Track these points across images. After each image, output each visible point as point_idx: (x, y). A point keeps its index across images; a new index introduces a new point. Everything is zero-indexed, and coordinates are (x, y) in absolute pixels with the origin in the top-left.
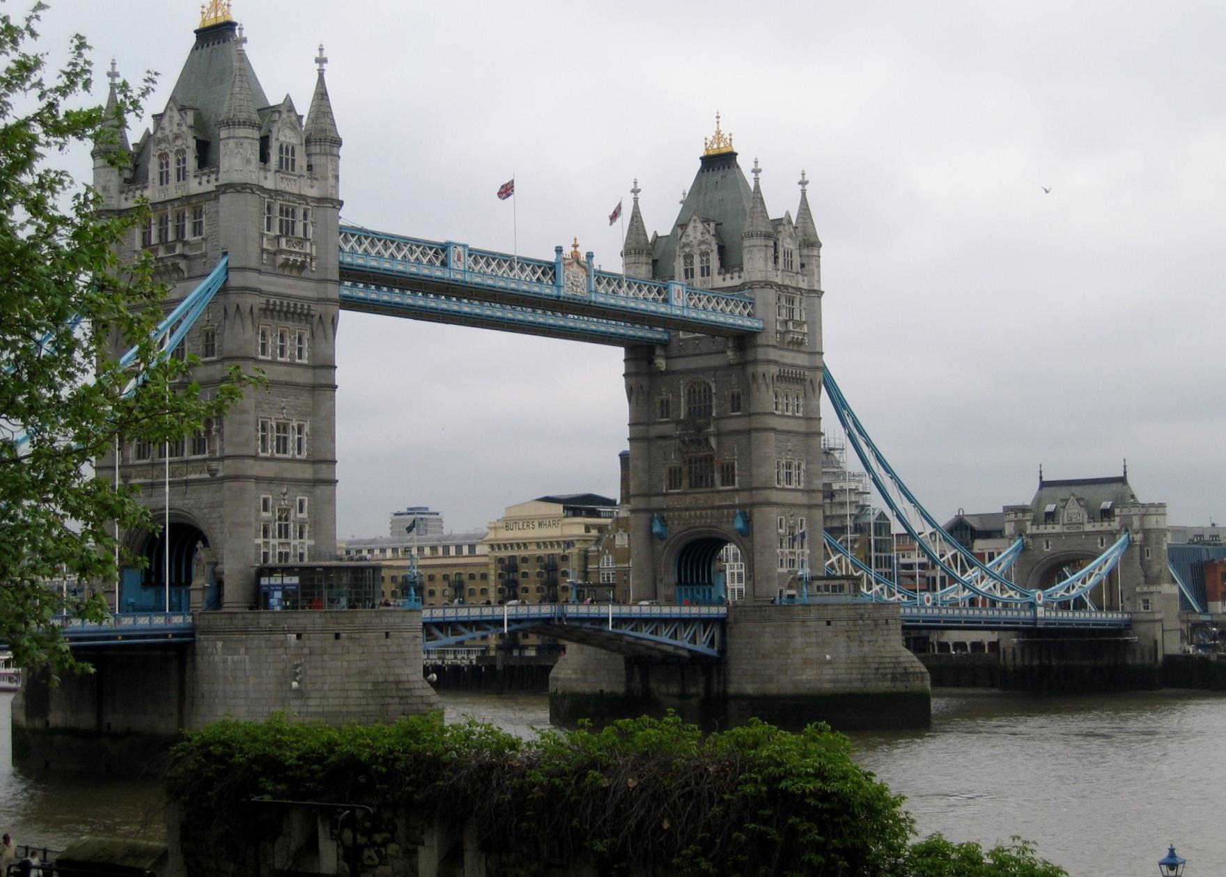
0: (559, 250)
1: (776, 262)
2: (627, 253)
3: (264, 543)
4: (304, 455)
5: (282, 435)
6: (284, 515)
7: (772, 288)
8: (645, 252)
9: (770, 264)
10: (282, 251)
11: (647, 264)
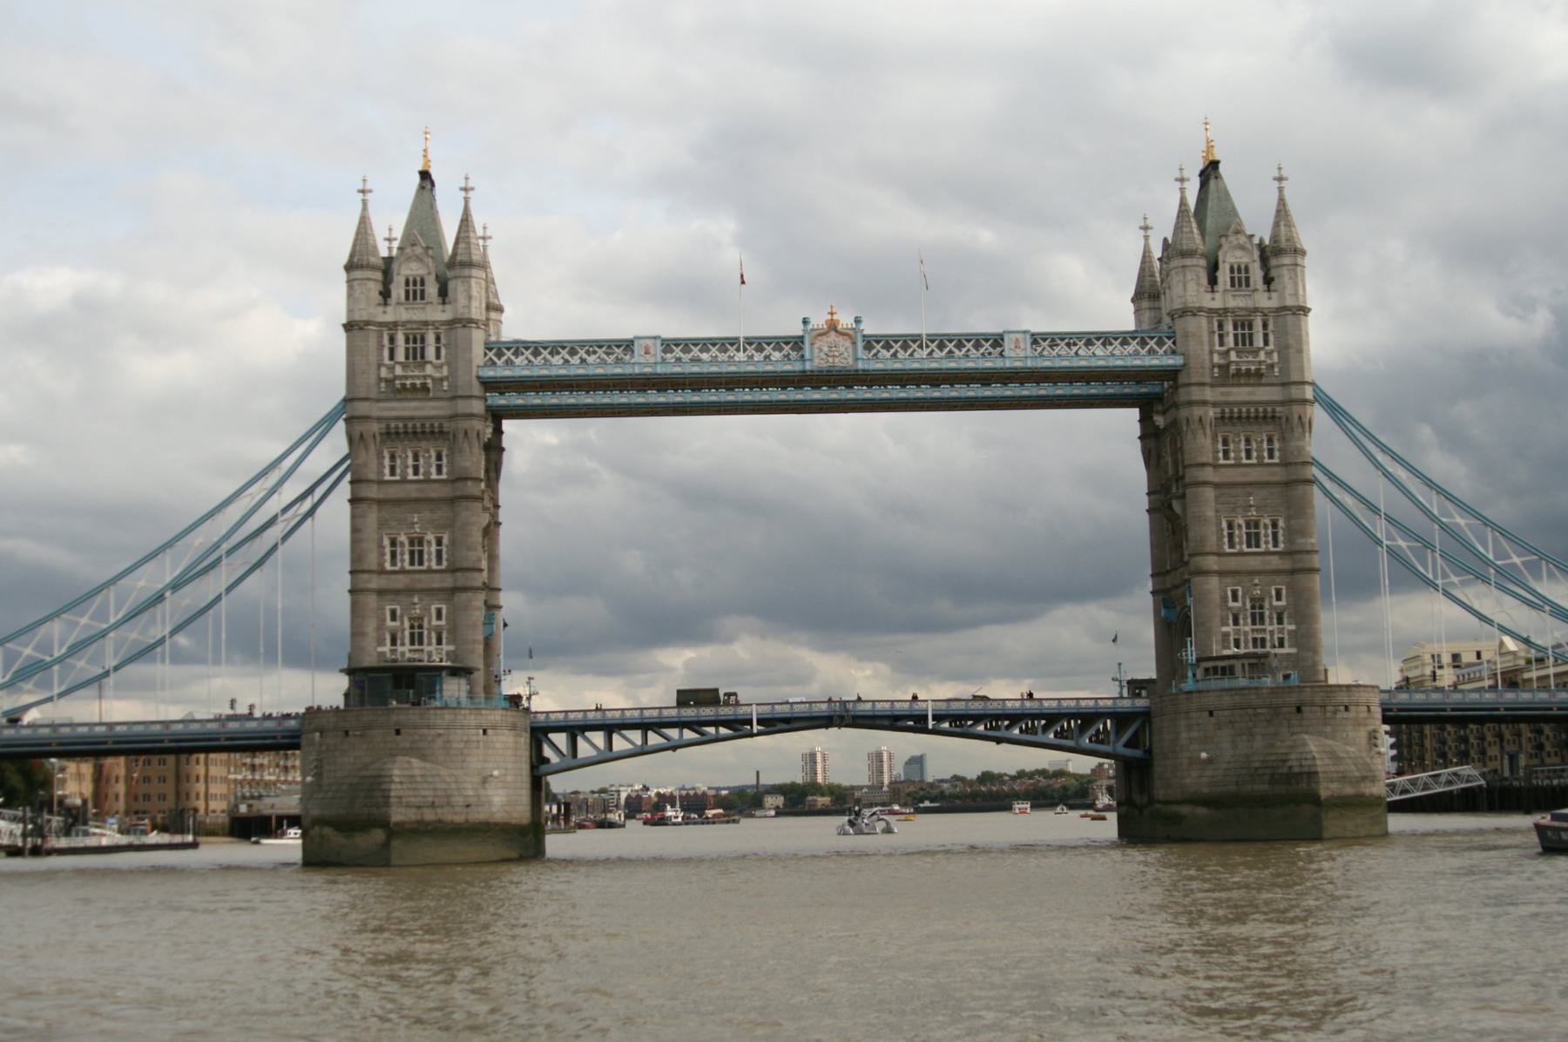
1: (1213, 281)
2: (1133, 300)
3: (391, 651)
4: (445, 564)
5: (416, 548)
6: (417, 623)
7: (1194, 315)
8: (1146, 295)
10: (396, 377)
11: (1150, 309)
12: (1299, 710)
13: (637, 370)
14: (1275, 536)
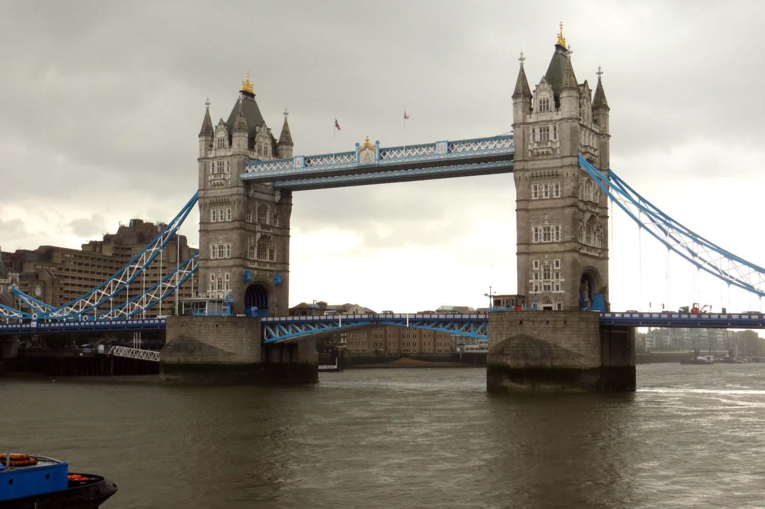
0: (357, 145)
1: (531, 110)
4: (230, 256)
9: (520, 113)
12: (521, 322)
13: (294, 171)
14: (557, 234)
